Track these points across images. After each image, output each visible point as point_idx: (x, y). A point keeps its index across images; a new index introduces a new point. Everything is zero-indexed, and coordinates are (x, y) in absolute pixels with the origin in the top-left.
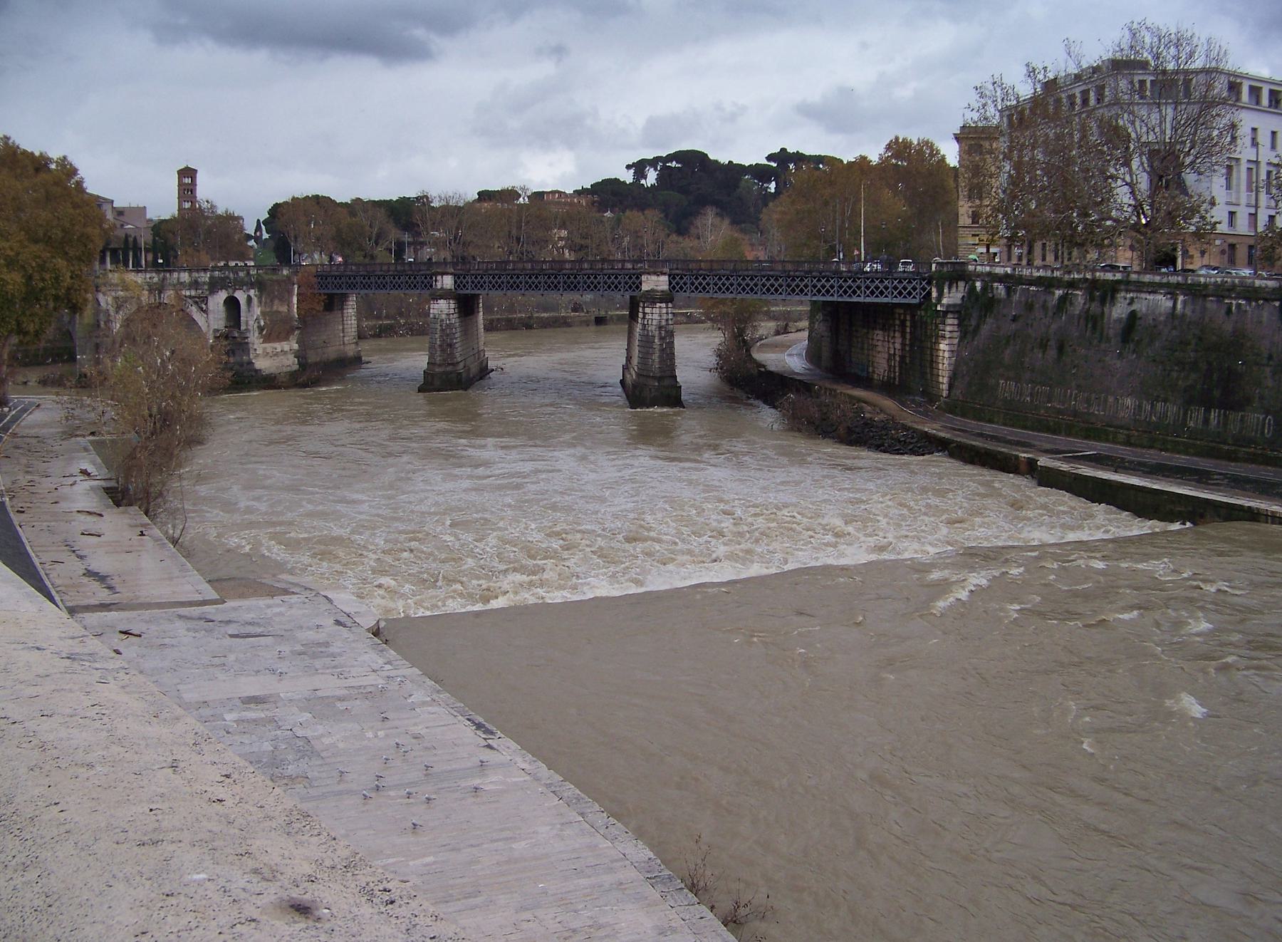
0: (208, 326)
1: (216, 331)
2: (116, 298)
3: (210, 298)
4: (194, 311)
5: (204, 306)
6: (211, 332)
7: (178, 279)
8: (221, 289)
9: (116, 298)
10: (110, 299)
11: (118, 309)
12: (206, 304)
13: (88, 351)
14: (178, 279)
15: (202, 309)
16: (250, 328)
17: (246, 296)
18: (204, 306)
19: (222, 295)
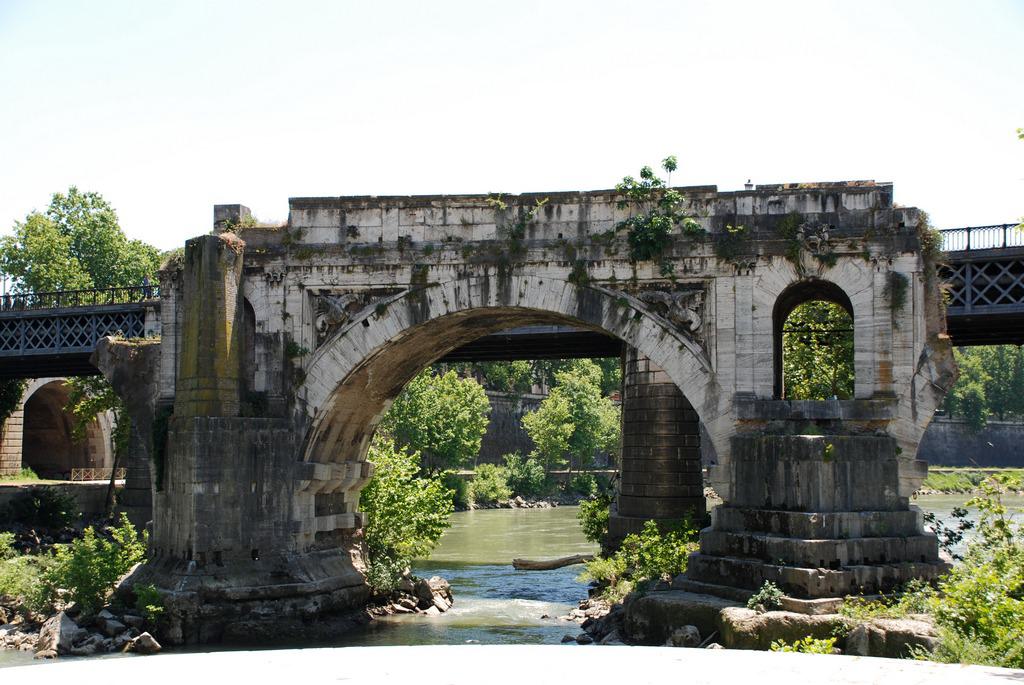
0: (712, 385)
1: (742, 400)
2: (321, 301)
5: (693, 316)
6: (724, 403)
7: (582, 225)
8: (769, 258)
9: (321, 301)
10: (297, 302)
11: (325, 336)
12: (700, 310)
13: (227, 472)
14: (582, 225)
15: (684, 327)
16: (900, 388)
17: (880, 280)
18: (693, 316)
19: (777, 276)
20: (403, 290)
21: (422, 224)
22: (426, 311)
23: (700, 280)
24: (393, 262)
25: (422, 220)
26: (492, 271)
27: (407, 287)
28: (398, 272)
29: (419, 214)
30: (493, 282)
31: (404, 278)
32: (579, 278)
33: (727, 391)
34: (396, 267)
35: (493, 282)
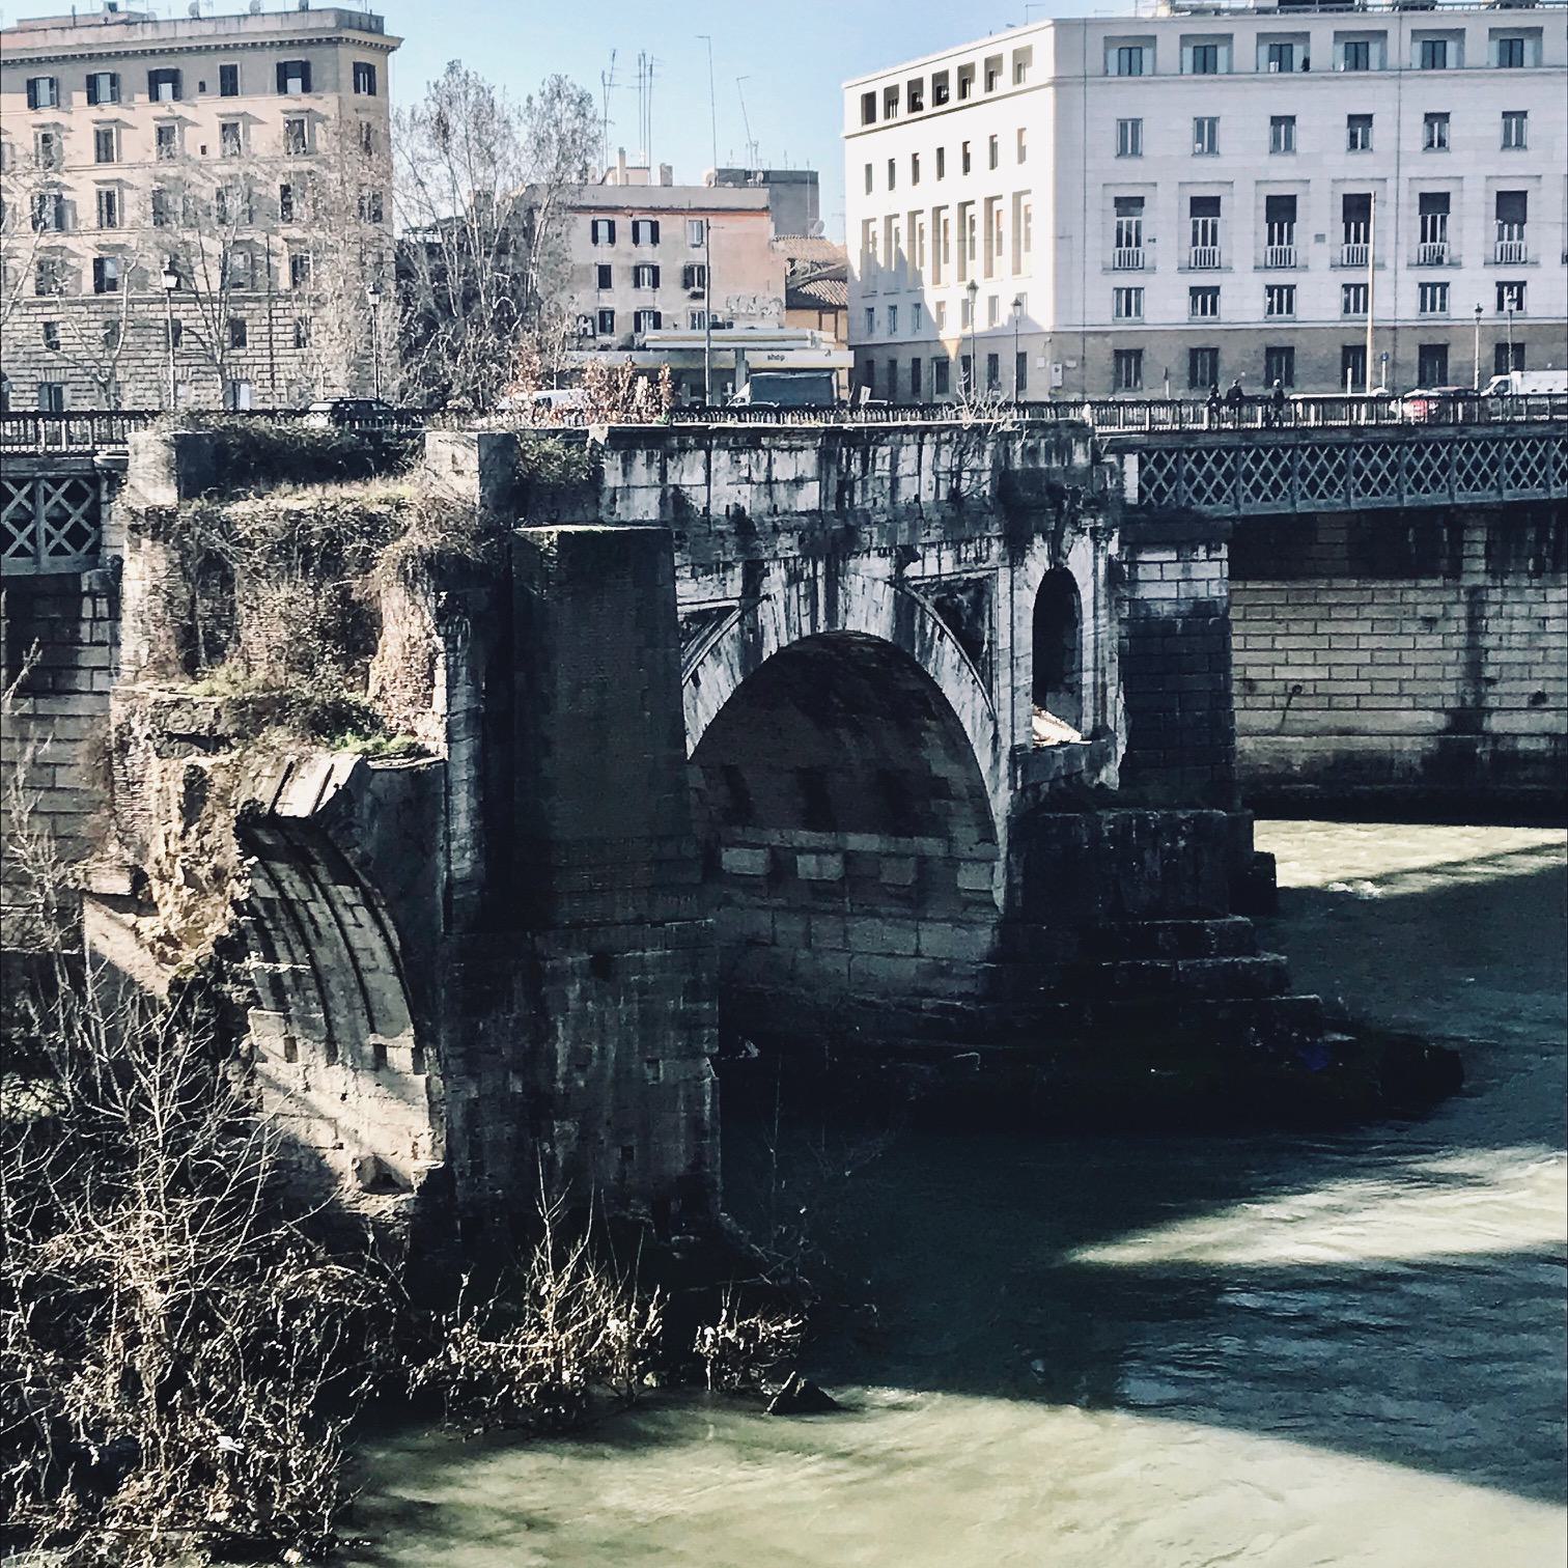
3: (1002, 586)
4: (947, 665)
6: (1004, 764)
20: (732, 608)
21: (748, 480)
22: (759, 643)
23: (986, 573)
24: (729, 558)
25: (745, 473)
26: (821, 566)
27: (735, 603)
28: (729, 574)
29: (744, 459)
30: (821, 584)
31: (735, 585)
32: (897, 581)
33: (1006, 742)
34: (728, 566)
35: (821, 584)
